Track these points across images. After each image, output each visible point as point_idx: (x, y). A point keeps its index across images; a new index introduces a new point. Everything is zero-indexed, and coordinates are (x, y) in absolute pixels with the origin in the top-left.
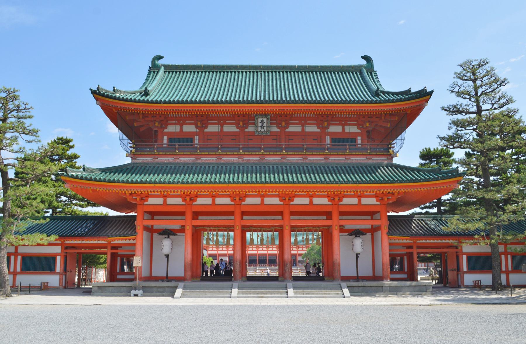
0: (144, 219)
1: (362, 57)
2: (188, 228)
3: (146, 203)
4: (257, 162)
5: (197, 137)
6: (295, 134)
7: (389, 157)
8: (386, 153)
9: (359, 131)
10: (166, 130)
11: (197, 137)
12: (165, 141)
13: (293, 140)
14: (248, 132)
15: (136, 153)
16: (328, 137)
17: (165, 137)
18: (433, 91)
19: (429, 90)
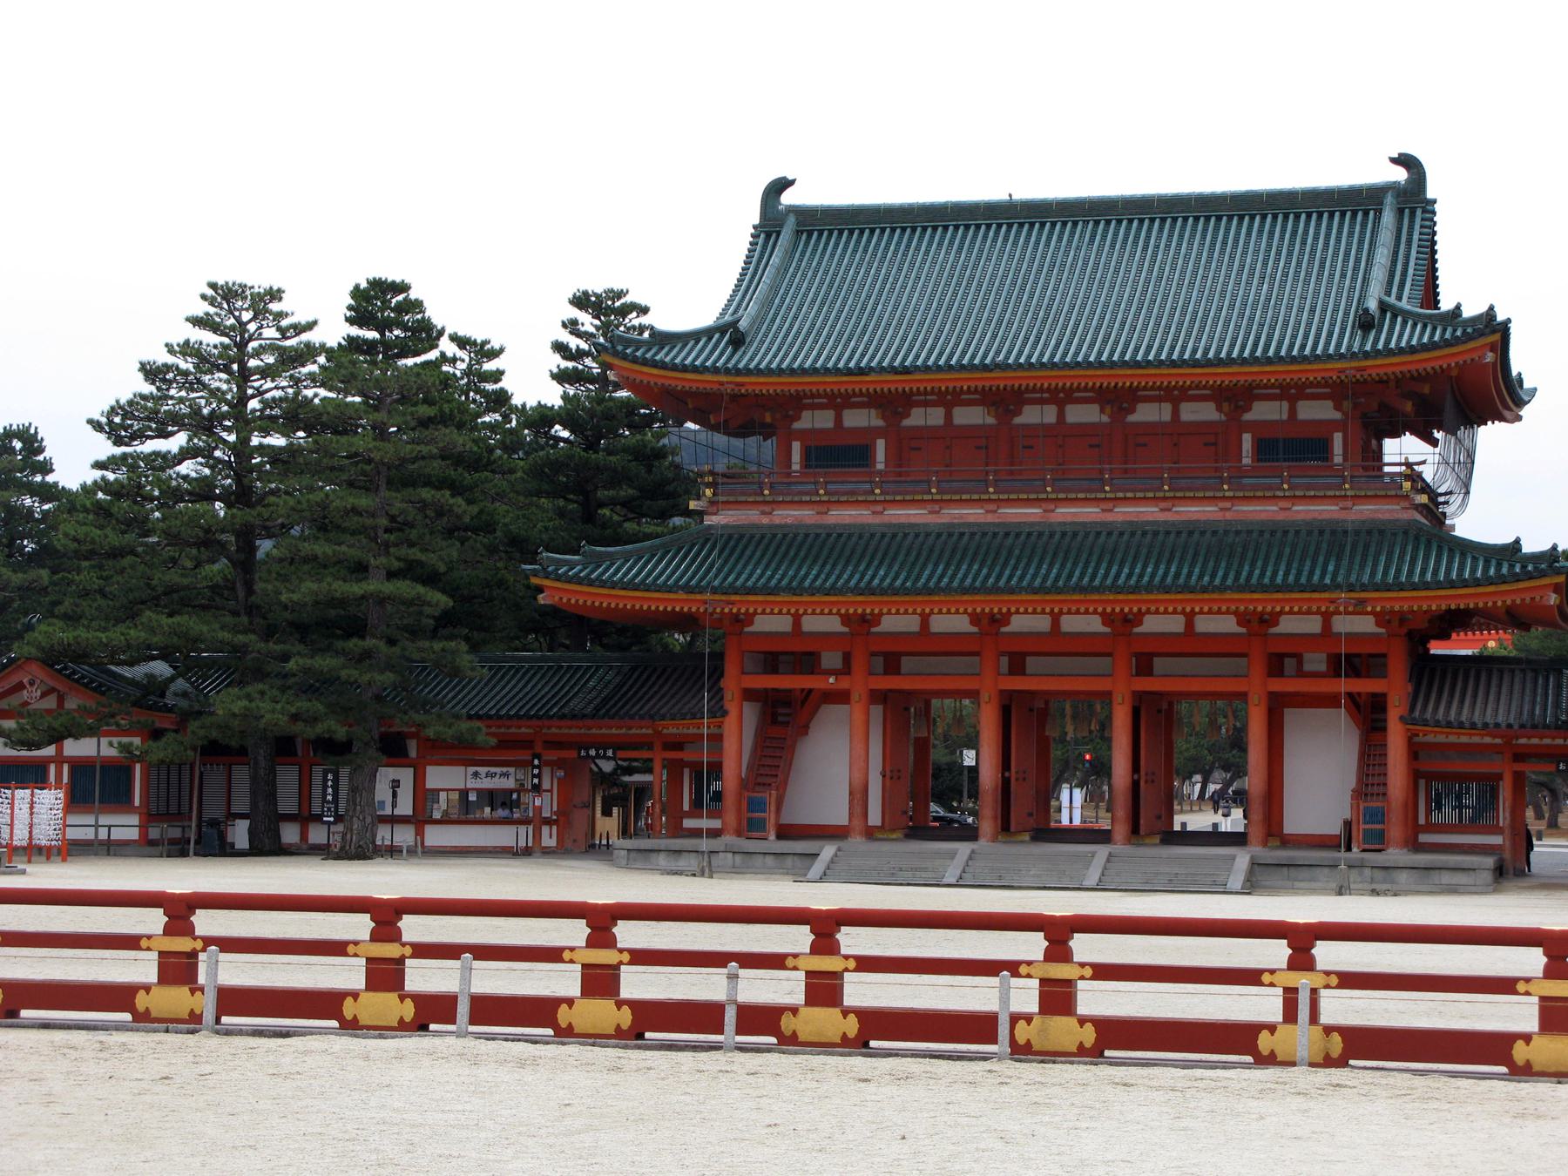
0: (743, 673)
1: (1394, 161)
2: (855, 696)
3: (746, 629)
4: (1031, 519)
5: (881, 445)
6: (1150, 429)
7: (1406, 504)
8: (1393, 493)
9: (1338, 416)
10: (797, 425)
11: (881, 445)
12: (796, 456)
13: (1145, 445)
14: (1023, 426)
15: (716, 498)
16: (1247, 440)
17: (796, 447)
18: (1509, 320)
19: (1500, 318)
